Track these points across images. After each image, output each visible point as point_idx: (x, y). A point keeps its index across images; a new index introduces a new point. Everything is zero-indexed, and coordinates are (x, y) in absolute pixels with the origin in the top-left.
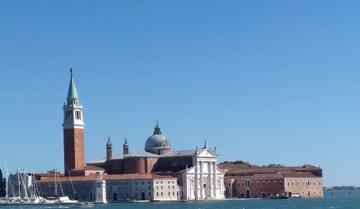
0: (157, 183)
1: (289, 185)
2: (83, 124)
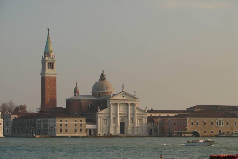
0: (61, 121)
1: (192, 124)
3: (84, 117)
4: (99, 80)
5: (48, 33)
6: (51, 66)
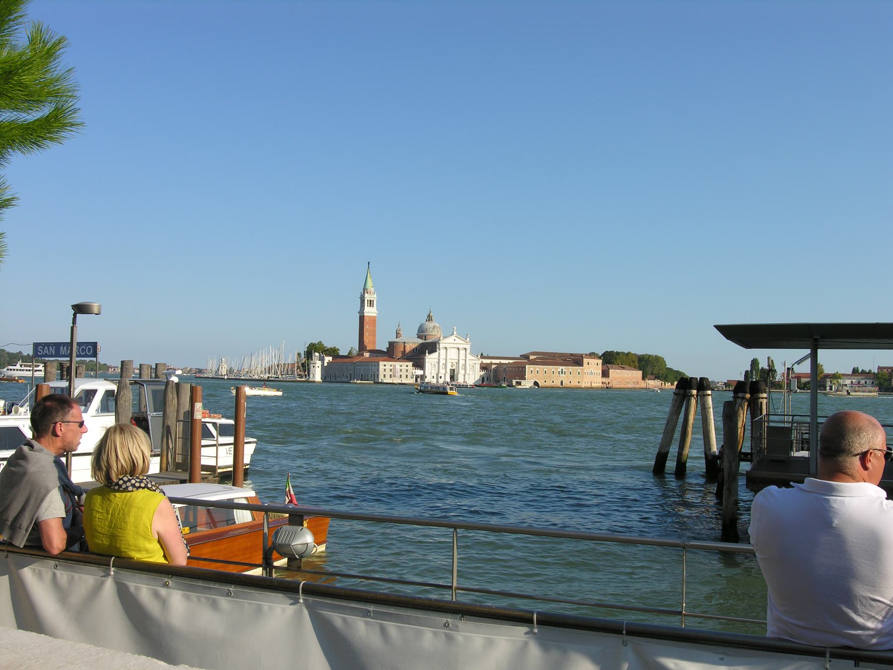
0: (385, 365)
1: (532, 373)
2: (376, 311)
3: (411, 361)
5: (369, 267)
6: (371, 303)
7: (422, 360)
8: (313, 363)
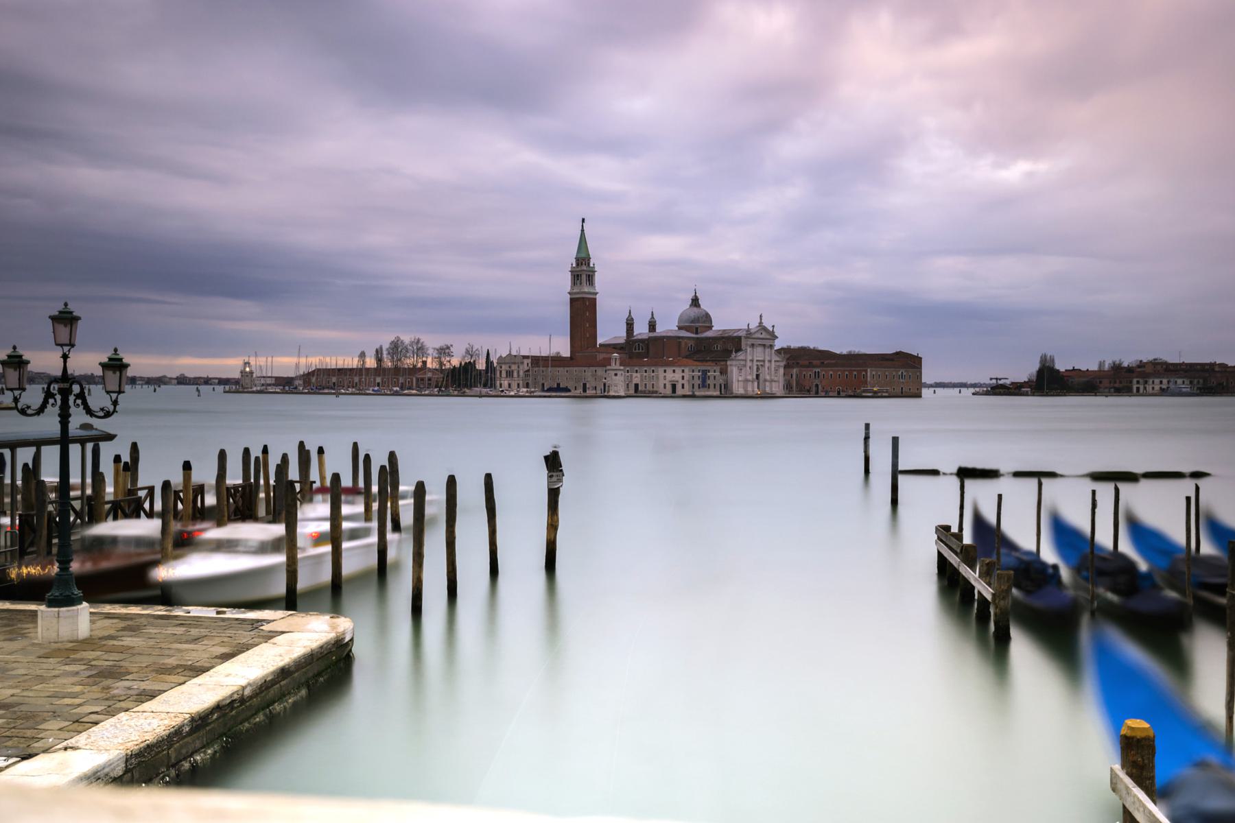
0: (693, 371)
4: (688, 307)
5: (583, 226)
6: (590, 279)
7: (722, 363)
8: (616, 370)
